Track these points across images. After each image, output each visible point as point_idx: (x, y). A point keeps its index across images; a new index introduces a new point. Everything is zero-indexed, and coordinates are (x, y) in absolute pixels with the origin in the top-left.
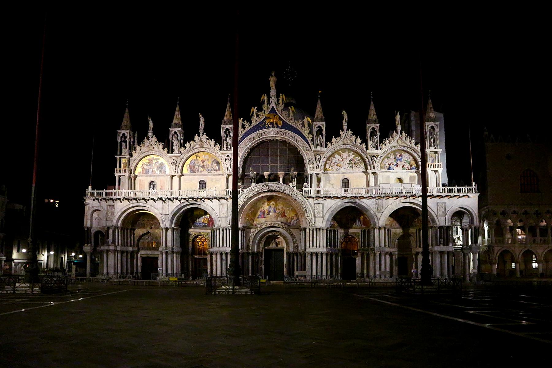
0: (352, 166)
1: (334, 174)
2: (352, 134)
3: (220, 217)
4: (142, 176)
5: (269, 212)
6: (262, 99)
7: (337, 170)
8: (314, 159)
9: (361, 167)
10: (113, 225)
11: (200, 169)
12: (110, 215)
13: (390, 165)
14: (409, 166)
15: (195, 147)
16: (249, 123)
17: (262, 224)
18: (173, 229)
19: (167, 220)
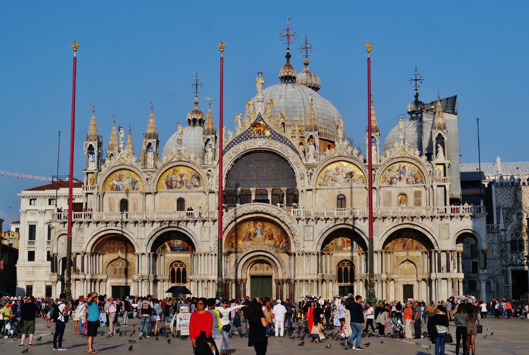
0: (349, 180)
1: (328, 189)
2: (348, 144)
3: (201, 241)
4: (112, 193)
5: (255, 235)
7: (332, 185)
8: (305, 173)
9: (359, 182)
11: (178, 185)
12: (79, 239)
13: (392, 178)
14: (414, 180)
15: (172, 161)
16: (232, 132)
17: (247, 248)
18: (149, 255)
19: (144, 245)
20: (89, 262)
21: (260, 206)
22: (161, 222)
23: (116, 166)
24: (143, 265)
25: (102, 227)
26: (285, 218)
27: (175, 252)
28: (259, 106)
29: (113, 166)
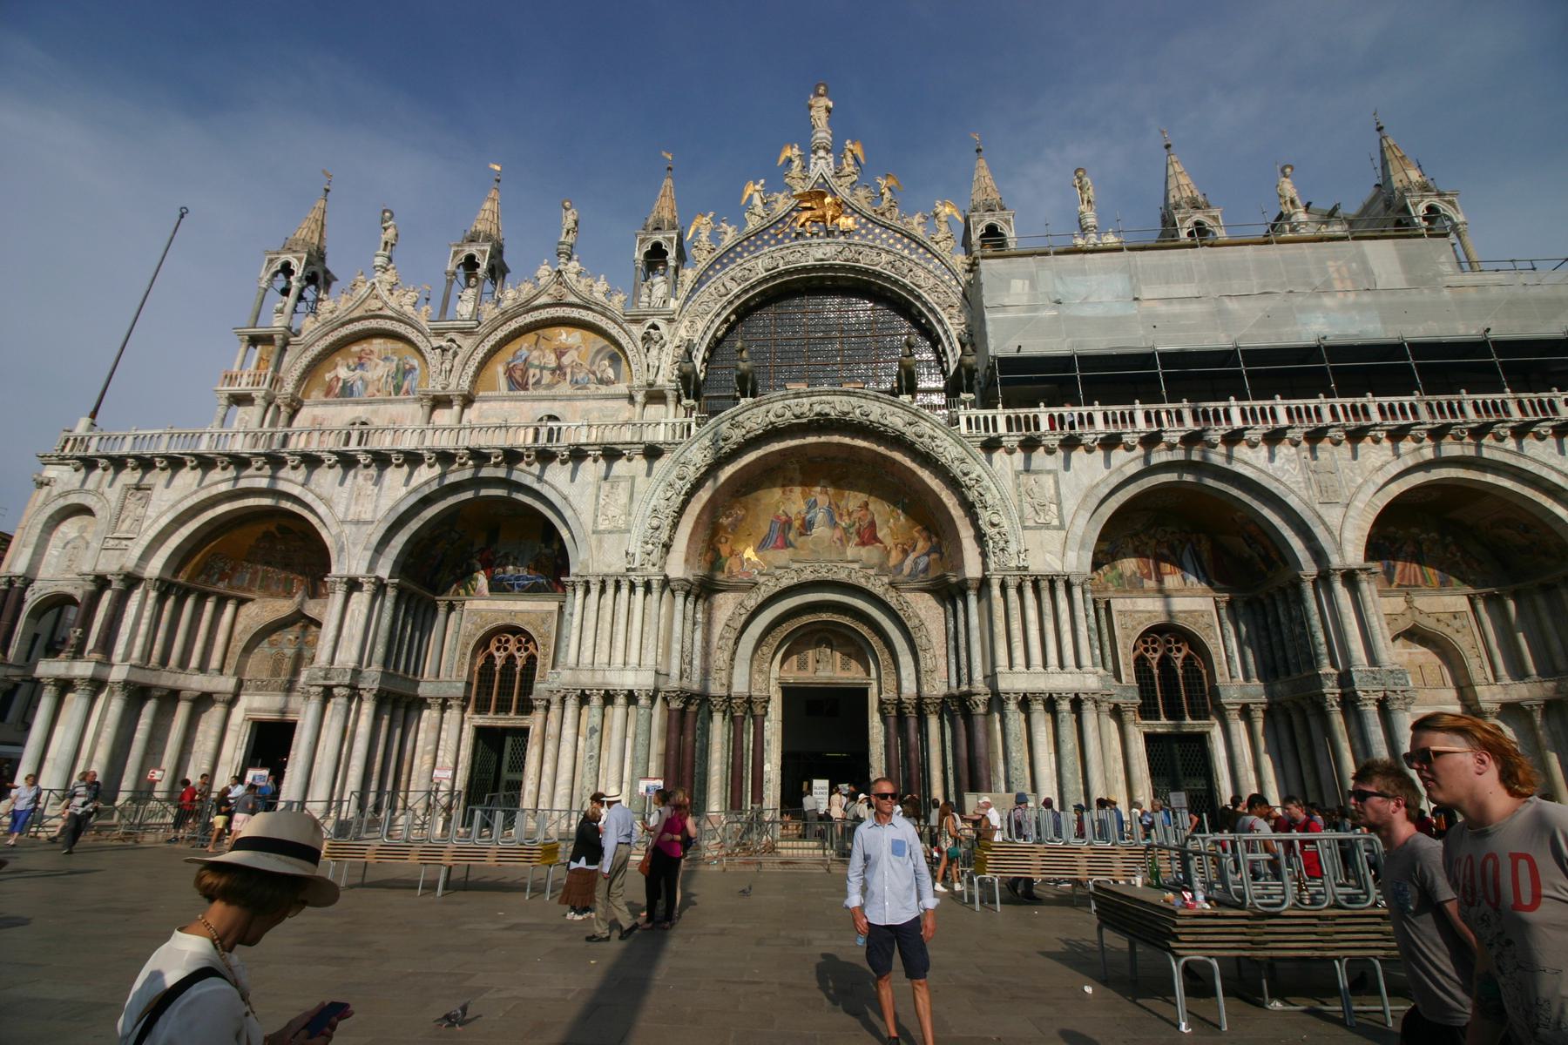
3: (594, 532)
4: (325, 404)
5: (807, 526)
6: (782, 158)
10: (120, 569)
15: (536, 303)
17: (778, 572)
19: (360, 548)
20: (147, 614)
21: (836, 399)
22: (445, 458)
23: (351, 321)
24: (350, 628)
25: (220, 480)
26: (938, 442)
27: (506, 595)
28: (819, 161)
29: (343, 320)
